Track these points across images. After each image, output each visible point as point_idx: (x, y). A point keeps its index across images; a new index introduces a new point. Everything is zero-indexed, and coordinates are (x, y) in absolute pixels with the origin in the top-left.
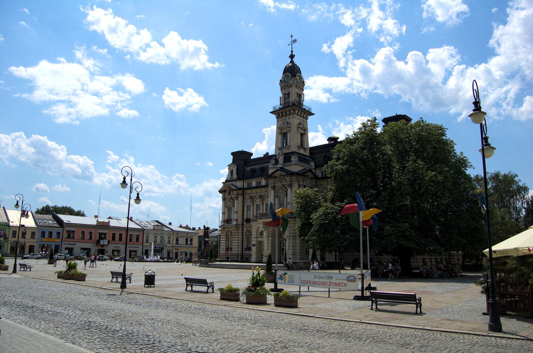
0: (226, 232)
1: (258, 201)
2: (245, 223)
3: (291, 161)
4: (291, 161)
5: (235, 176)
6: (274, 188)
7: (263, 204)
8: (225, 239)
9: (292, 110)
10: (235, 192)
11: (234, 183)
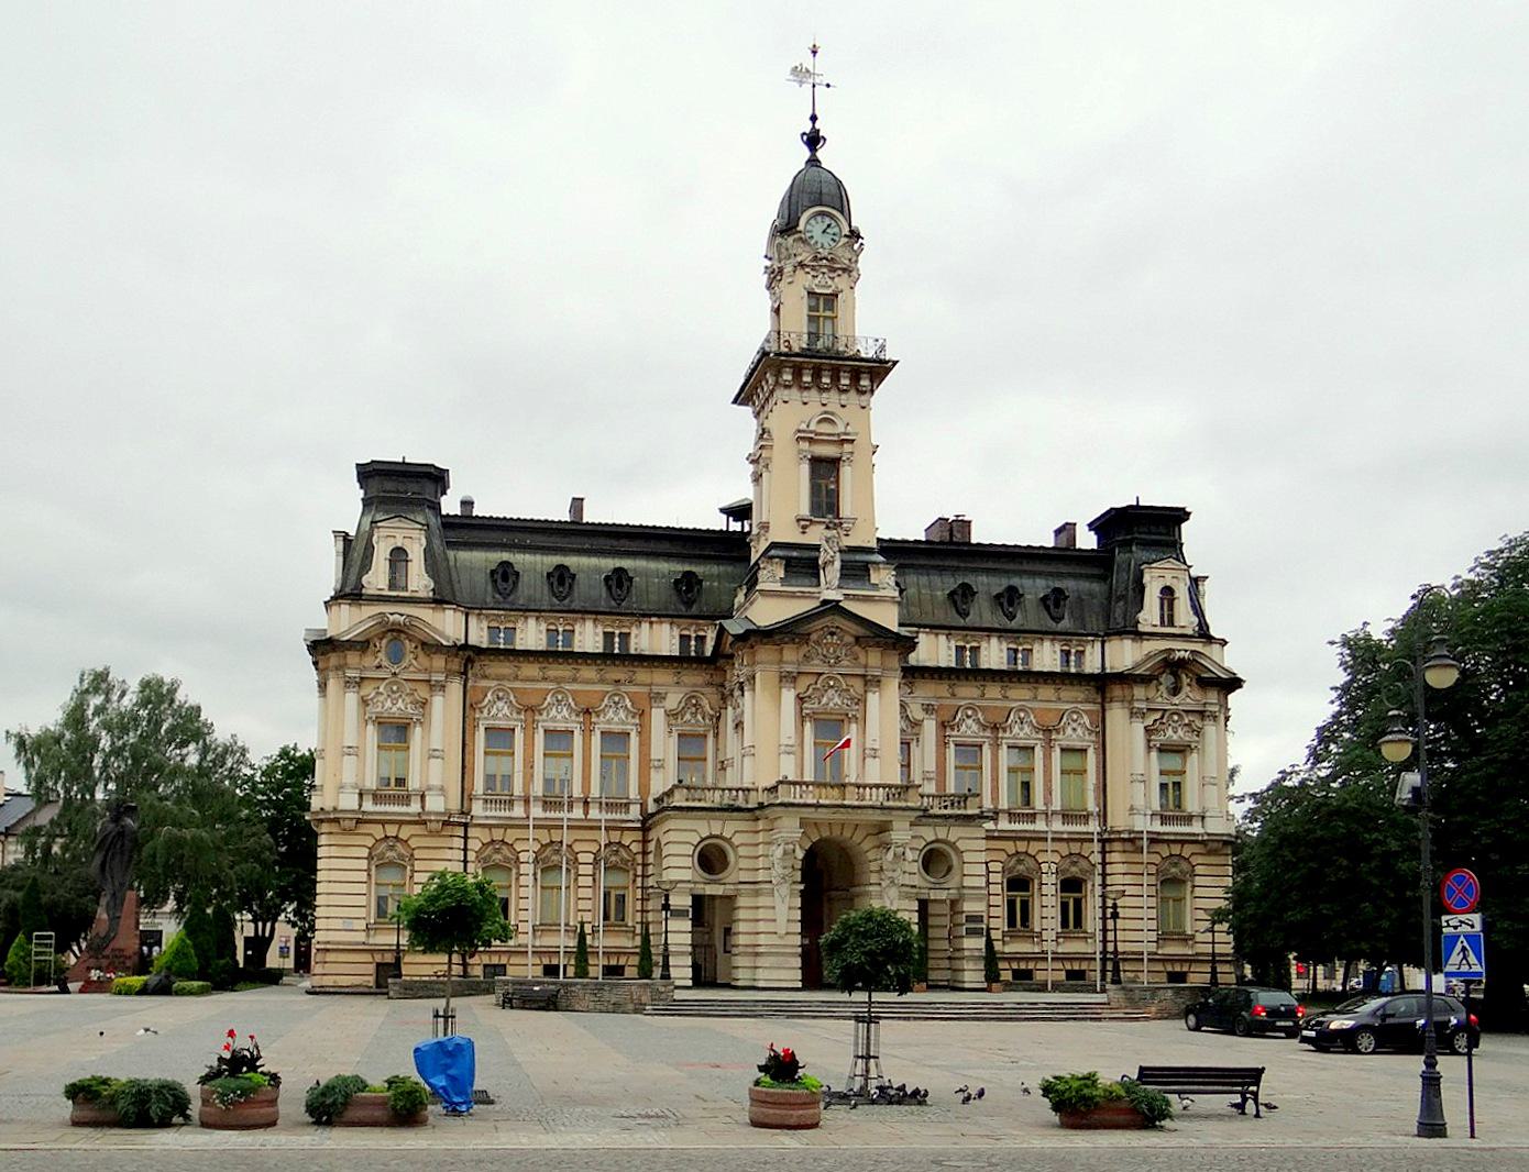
0: (370, 842)
1: (560, 716)
2: (478, 809)
4: (875, 587)
5: (419, 580)
6: (789, 678)
10: (439, 662)
11: (425, 614)
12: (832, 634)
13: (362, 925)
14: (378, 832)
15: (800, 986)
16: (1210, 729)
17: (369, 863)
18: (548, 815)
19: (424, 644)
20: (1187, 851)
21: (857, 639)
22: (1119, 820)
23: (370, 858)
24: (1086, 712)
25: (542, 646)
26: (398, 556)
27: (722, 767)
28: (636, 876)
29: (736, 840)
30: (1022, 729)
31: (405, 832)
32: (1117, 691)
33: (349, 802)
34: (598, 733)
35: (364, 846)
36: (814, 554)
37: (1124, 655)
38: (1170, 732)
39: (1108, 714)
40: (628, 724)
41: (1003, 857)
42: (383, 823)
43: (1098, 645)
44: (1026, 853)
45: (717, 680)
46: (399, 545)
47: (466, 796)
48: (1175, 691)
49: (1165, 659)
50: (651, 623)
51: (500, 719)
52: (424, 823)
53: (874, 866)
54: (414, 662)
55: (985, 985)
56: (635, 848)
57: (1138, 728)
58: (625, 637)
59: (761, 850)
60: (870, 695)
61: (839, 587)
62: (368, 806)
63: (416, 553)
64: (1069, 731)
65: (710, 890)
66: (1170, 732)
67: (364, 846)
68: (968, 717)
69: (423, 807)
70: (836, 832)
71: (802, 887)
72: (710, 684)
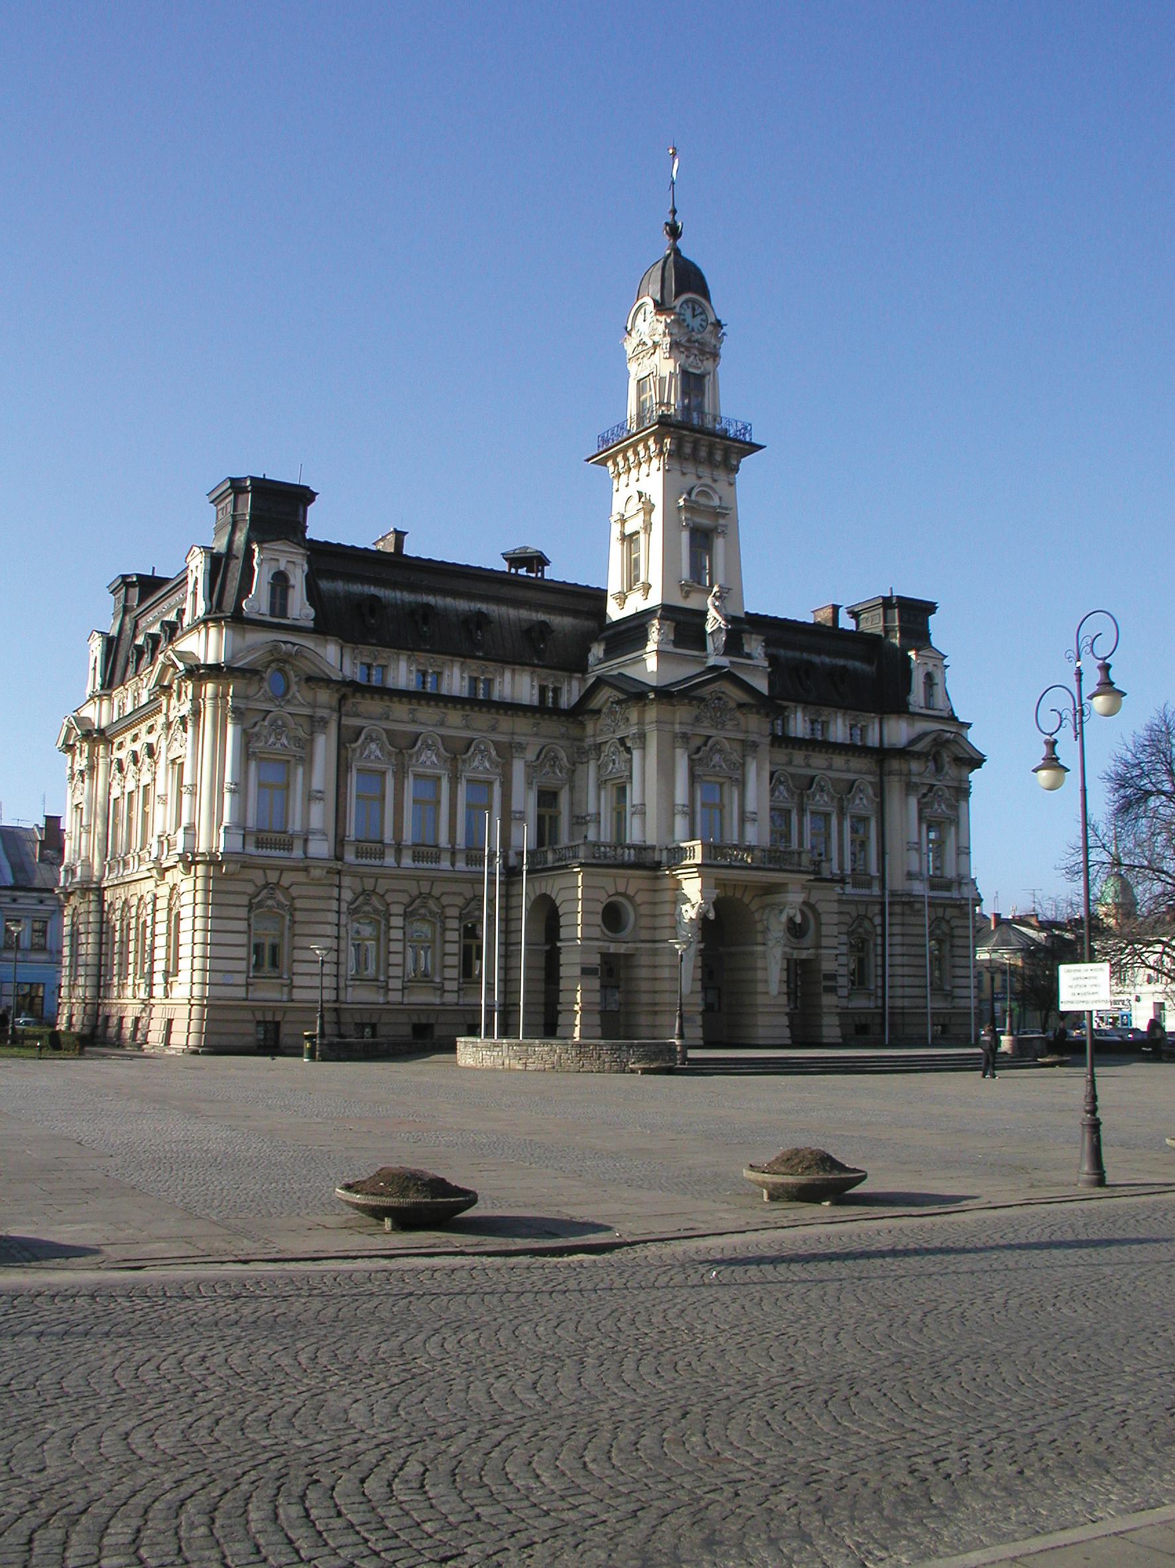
0: (251, 889)
1: (428, 760)
2: (350, 857)
3: (749, 656)
4: (749, 656)
5: (299, 607)
7: (454, 781)
8: (242, 926)
10: (325, 696)
11: (308, 642)
12: (719, 699)
13: (241, 979)
14: (258, 876)
15: (701, 1043)
16: (963, 803)
17: (249, 911)
18: (417, 864)
19: (309, 679)
20: (950, 912)
21: (741, 706)
22: (896, 881)
23: (250, 907)
24: (870, 783)
25: (413, 686)
26: (280, 582)
27: (579, 821)
29: (639, 899)
30: (821, 796)
32: (895, 764)
34: (464, 782)
35: (244, 893)
36: (697, 620)
37: (899, 732)
38: (936, 806)
39: (886, 786)
40: (492, 773)
41: (847, 919)
42: (264, 868)
43: (877, 721)
44: (865, 916)
45: (575, 731)
46: (282, 568)
47: (340, 841)
48: (939, 769)
49: (935, 739)
50: (513, 671)
51: (372, 762)
52: (306, 869)
53: (759, 927)
54: (298, 695)
55: (840, 1040)
57: (913, 802)
58: (489, 683)
60: (749, 759)
61: (725, 654)
62: (251, 849)
63: (298, 579)
64: (857, 801)
65: (613, 948)
66: (936, 806)
67: (244, 893)
68: (781, 783)
69: (305, 852)
70: (730, 894)
71: (702, 946)
72: (563, 736)
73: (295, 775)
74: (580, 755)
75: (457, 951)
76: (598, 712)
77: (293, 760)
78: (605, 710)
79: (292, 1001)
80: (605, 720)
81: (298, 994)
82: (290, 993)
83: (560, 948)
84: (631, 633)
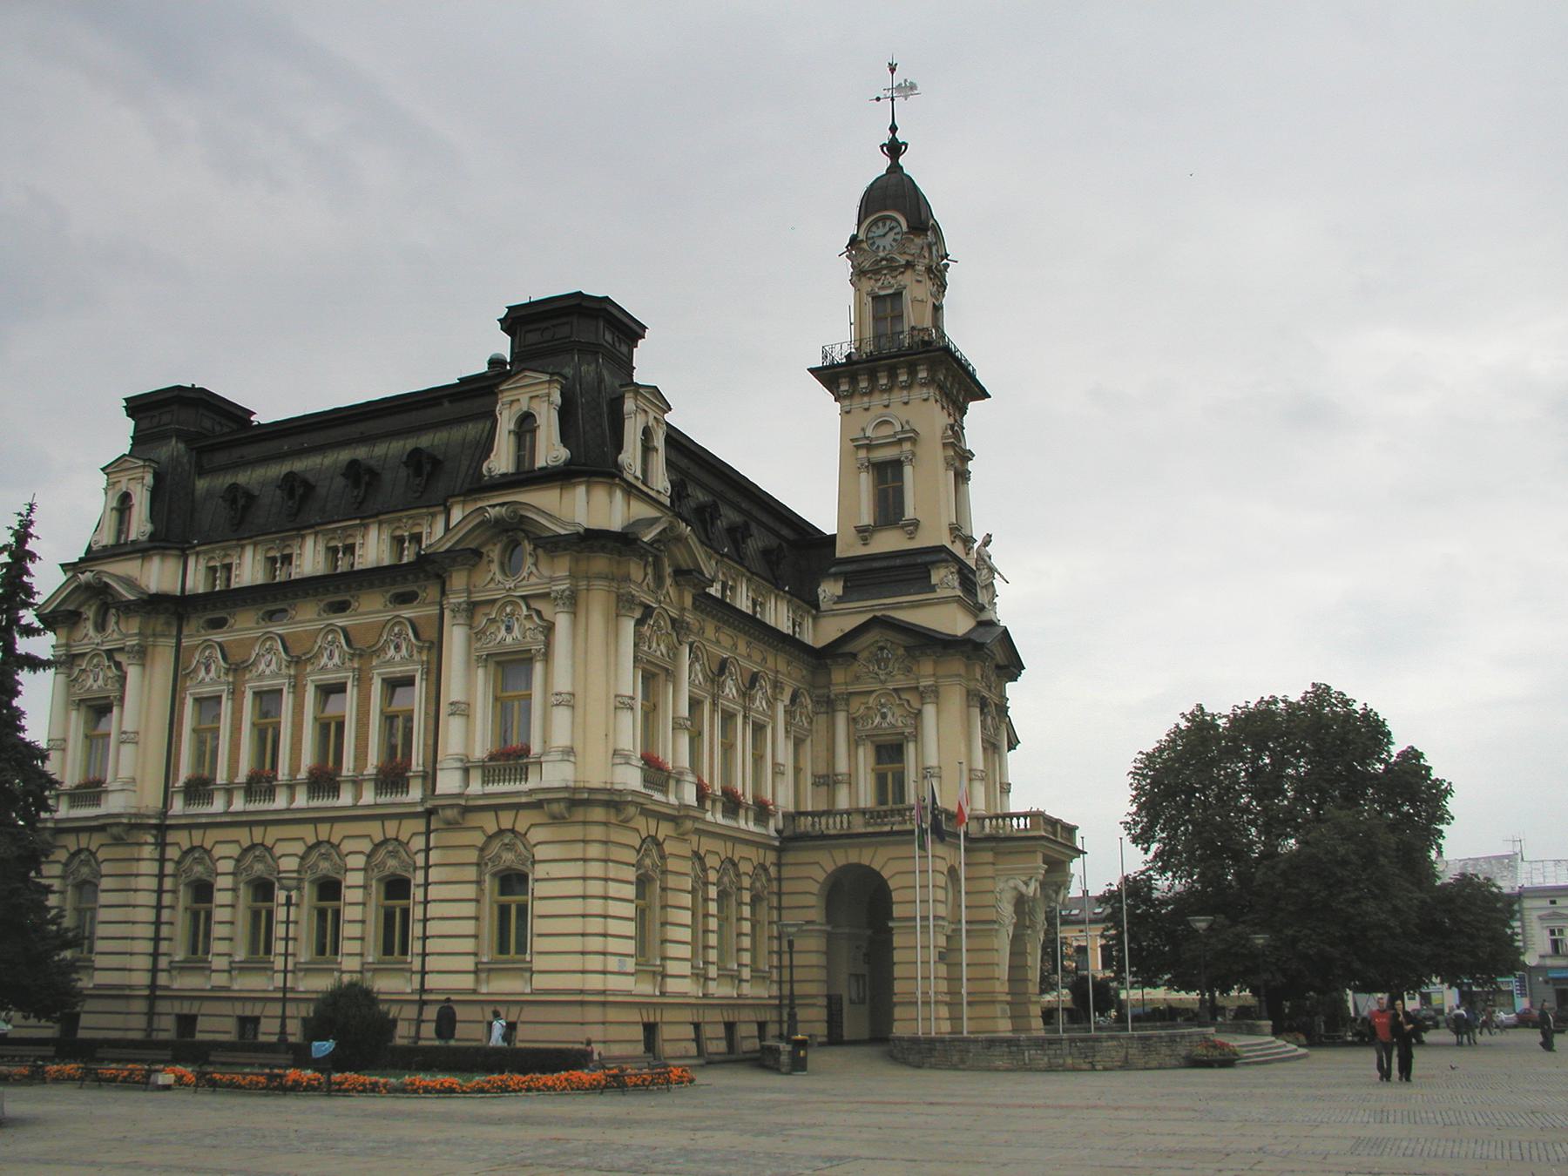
5: (661, 482)
9: (903, 365)
14: (640, 822)
27: (828, 781)
28: (771, 908)
31: (665, 830)
33: (631, 778)
56: (773, 871)
59: (987, 885)
63: (659, 441)
73: (666, 693)
74: (828, 705)
75: (633, 933)
76: (854, 656)
77: (662, 676)
78: (863, 656)
79: (663, 994)
80: (857, 667)
81: (673, 986)
82: (662, 984)
83: (892, 929)
84: (912, 570)
